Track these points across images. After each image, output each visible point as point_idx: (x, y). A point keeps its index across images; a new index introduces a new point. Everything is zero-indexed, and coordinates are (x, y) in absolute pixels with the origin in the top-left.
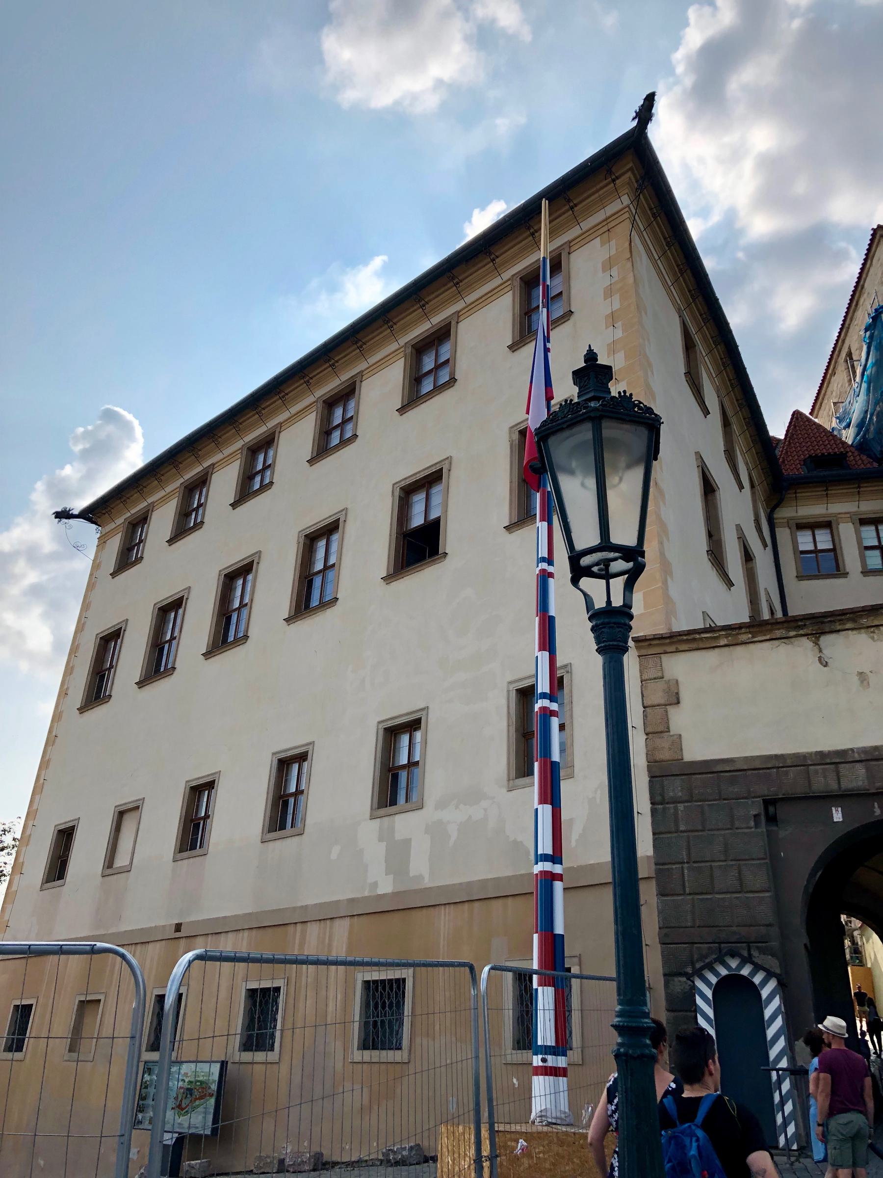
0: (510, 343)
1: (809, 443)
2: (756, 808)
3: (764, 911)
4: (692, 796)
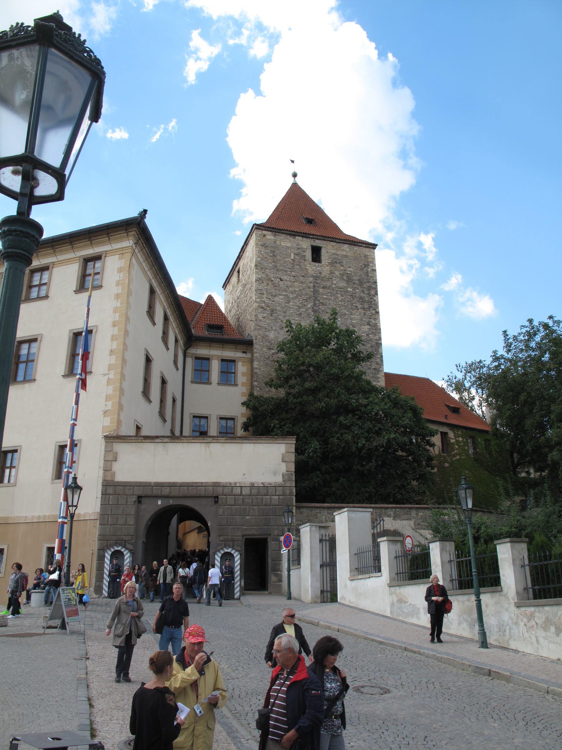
0: (74, 289)
1: (211, 315)
2: (134, 499)
3: (132, 531)
4: (115, 492)
